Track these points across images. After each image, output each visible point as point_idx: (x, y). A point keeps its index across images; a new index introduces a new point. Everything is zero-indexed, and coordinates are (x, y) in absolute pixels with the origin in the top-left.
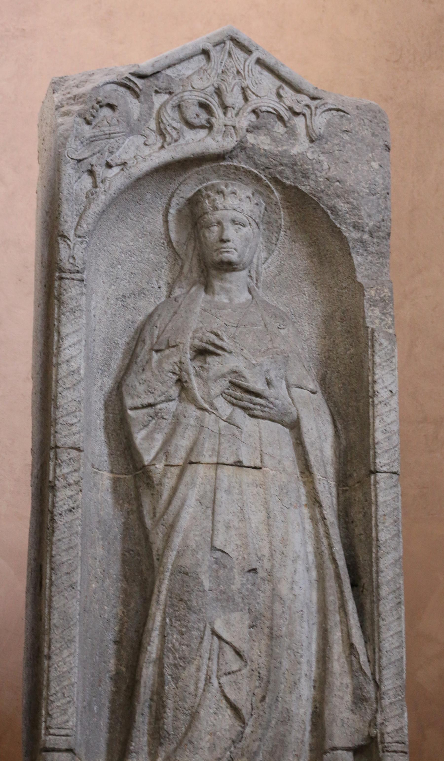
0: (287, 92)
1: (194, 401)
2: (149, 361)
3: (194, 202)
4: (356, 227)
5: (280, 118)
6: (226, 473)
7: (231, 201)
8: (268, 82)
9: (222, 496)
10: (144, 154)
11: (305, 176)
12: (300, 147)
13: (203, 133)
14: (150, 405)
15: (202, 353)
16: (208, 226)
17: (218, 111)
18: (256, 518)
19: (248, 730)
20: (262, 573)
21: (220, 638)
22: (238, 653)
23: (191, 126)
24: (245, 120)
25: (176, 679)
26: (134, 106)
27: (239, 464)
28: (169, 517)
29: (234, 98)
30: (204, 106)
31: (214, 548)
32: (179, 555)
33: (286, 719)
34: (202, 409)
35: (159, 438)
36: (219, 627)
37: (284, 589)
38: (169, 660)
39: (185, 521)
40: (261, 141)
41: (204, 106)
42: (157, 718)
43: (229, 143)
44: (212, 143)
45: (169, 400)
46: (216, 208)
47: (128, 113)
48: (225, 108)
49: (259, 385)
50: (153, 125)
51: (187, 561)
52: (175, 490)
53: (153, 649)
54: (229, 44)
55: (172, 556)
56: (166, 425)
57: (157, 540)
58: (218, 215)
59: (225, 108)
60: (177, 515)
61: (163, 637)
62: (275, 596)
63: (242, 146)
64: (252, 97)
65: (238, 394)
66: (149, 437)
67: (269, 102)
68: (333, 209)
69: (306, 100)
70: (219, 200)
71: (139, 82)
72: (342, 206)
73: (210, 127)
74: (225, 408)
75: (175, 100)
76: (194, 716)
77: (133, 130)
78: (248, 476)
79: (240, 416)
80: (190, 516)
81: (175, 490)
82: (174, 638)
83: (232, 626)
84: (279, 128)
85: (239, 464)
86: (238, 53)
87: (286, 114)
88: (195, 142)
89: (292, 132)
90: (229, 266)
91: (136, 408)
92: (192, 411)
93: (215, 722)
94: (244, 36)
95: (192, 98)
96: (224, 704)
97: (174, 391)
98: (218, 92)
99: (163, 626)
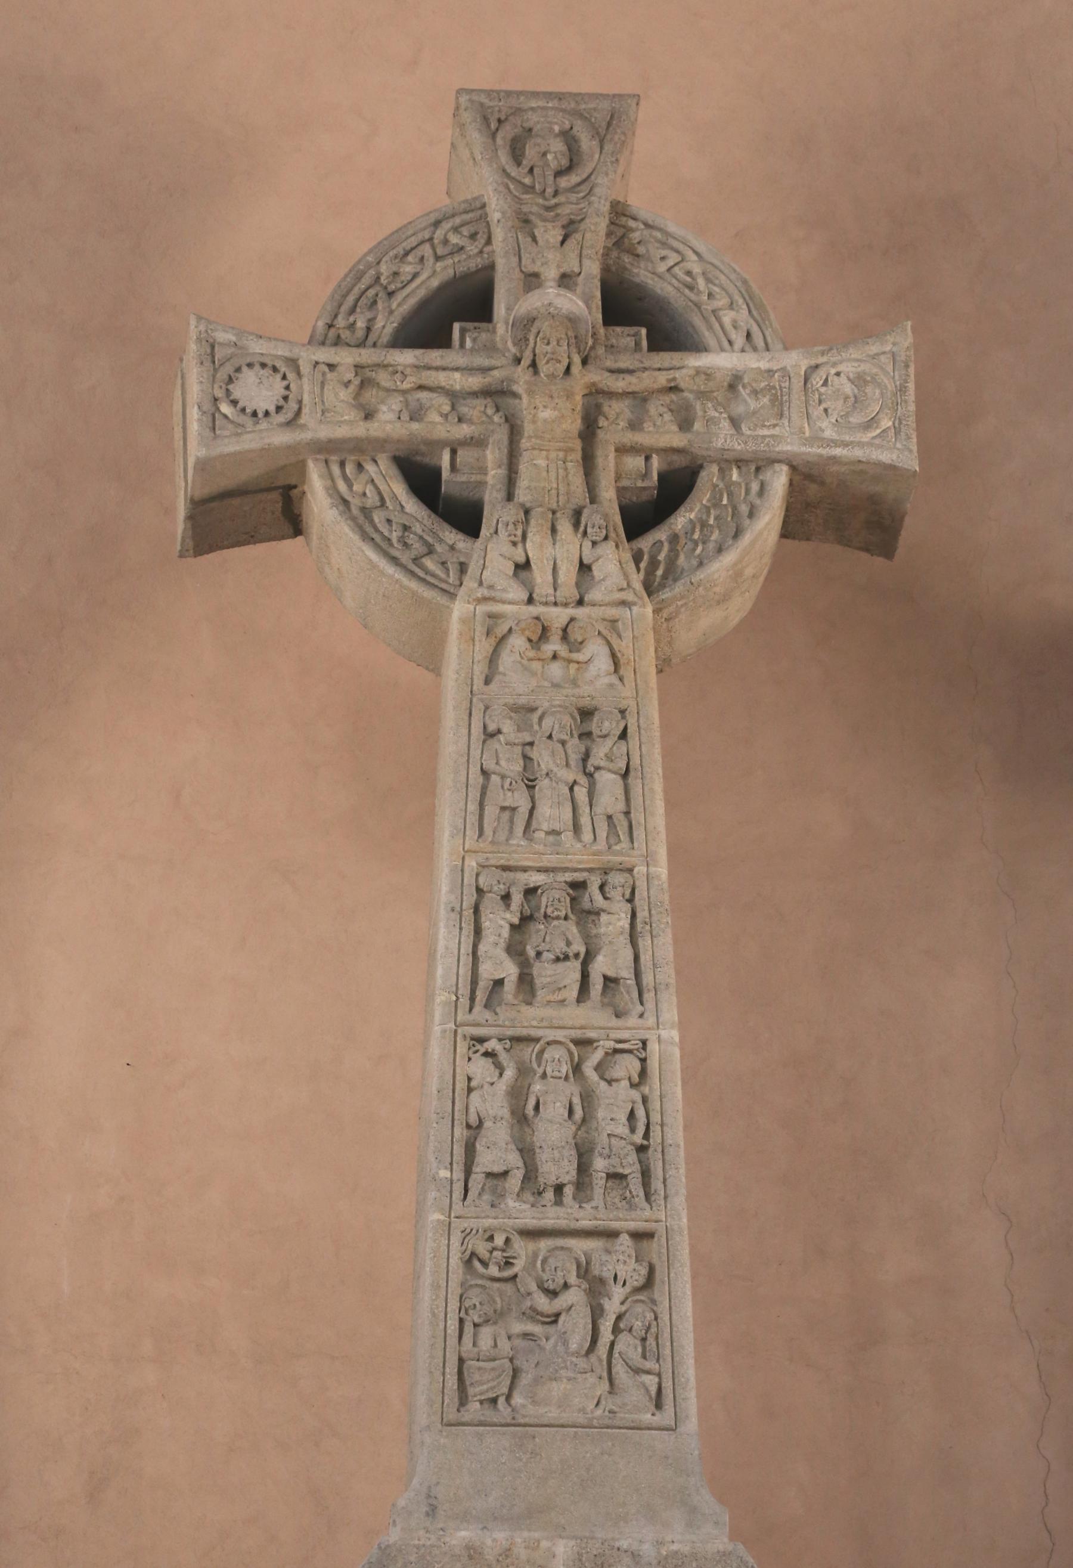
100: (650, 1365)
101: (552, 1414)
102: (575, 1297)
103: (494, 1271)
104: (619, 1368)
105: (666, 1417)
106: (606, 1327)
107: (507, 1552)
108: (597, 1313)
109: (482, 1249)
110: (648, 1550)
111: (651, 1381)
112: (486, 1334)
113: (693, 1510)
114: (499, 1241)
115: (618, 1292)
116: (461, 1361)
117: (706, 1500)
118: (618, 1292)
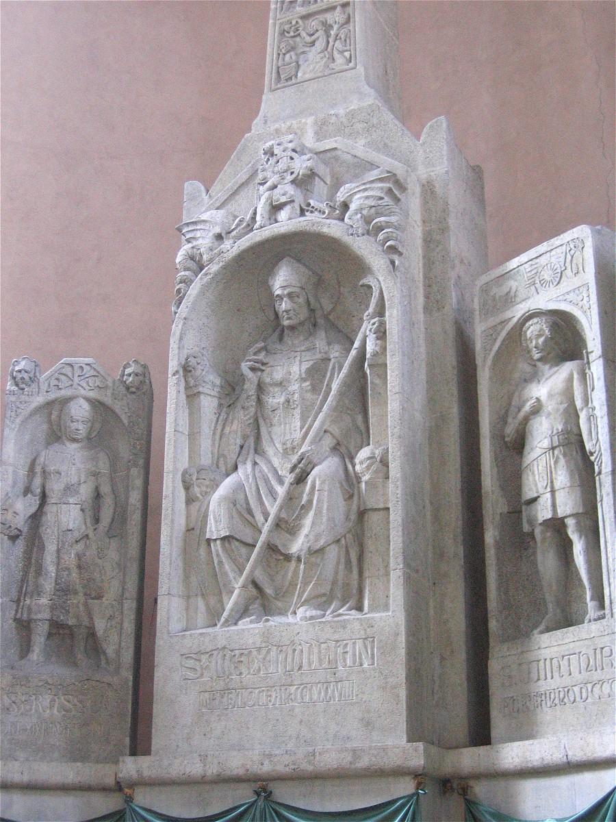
100: (348, 48)
101: (307, 76)
102: (320, 33)
103: (292, 34)
104: (335, 52)
105: (351, 65)
106: (331, 40)
107: (289, 128)
108: (328, 36)
109: (286, 27)
110: (342, 112)
111: (347, 54)
112: (288, 56)
113: (361, 93)
114: (294, 22)
115: (336, 27)
116: (278, 68)
117: (366, 89)
118: (336, 27)
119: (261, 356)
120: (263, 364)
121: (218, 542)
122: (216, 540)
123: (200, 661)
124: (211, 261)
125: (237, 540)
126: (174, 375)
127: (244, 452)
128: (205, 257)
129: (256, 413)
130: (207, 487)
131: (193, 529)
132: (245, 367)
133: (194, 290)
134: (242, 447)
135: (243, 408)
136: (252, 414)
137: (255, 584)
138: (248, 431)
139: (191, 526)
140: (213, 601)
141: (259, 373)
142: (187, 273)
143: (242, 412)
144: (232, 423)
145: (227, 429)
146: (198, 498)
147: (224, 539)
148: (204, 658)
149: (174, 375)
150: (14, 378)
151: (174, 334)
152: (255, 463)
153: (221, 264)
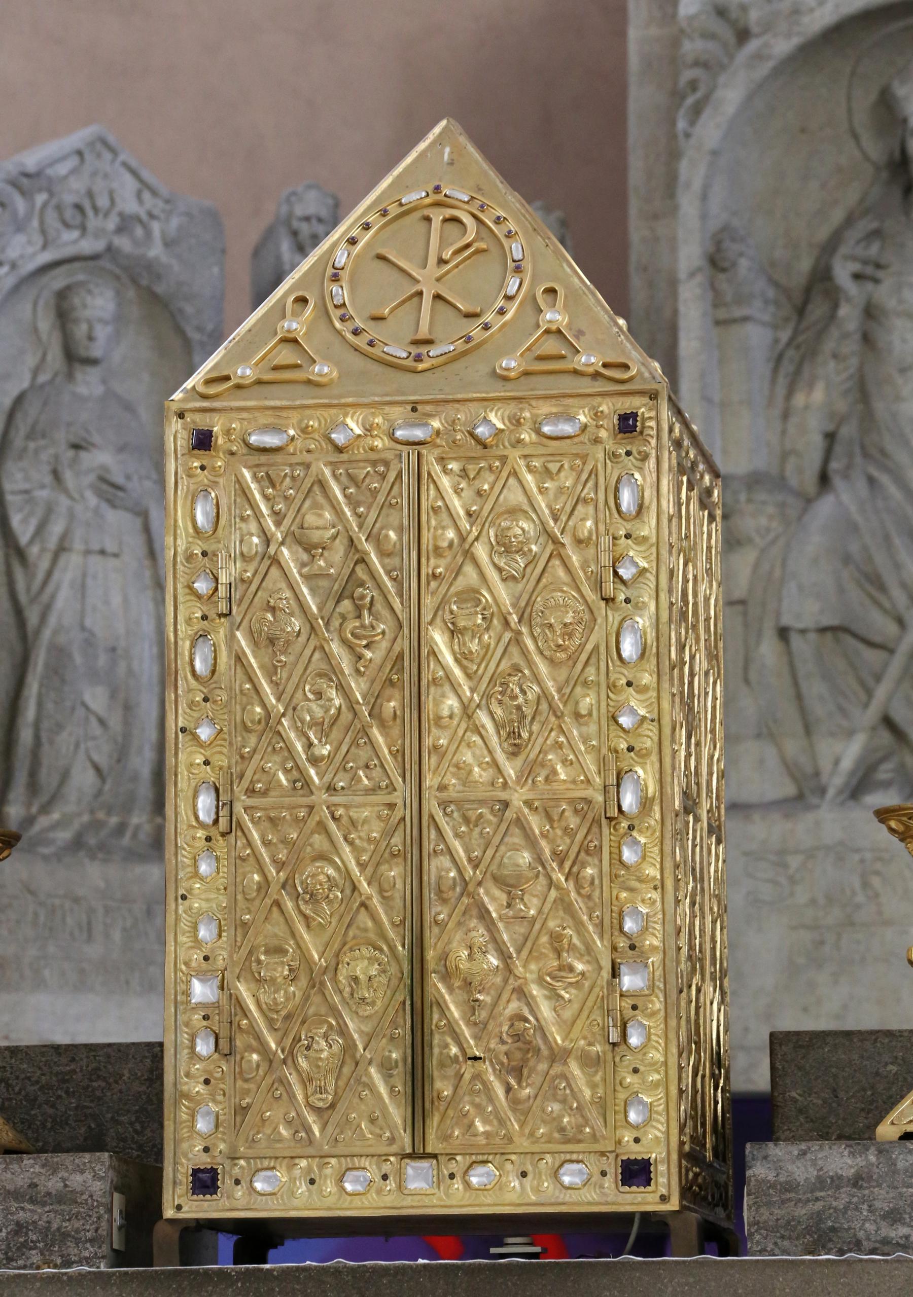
0: (146, 195)
1: (66, 491)
2: (25, 449)
3: (62, 295)
4: (199, 329)
5: (140, 221)
6: (95, 560)
7: (99, 302)
8: (129, 184)
9: (90, 582)
10: (25, 250)
11: (159, 277)
12: (156, 251)
13: (75, 234)
14: (26, 492)
15: (76, 447)
16: (76, 321)
17: (90, 213)
18: (116, 600)
19: (107, 787)
20: (119, 652)
21: (87, 708)
22: (102, 722)
23: (67, 225)
24: (111, 224)
25: (51, 742)
26: (20, 204)
27: (102, 552)
28: (45, 597)
29: (103, 202)
30: (79, 207)
31: (83, 628)
32: (56, 632)
33: (135, 778)
34: (72, 498)
35: (33, 523)
36: (87, 698)
37: (135, 665)
38: (45, 725)
39: (59, 603)
40: (124, 243)
41: (79, 207)
42: (33, 774)
43: (99, 246)
44: (88, 246)
45: (43, 487)
46: (85, 306)
47: (15, 213)
48: (96, 209)
49: (120, 480)
50: (35, 223)
51: (62, 639)
52: (49, 574)
53: (30, 712)
54: (99, 146)
55: (47, 633)
56: (40, 512)
57: (32, 618)
58: (87, 313)
59: (96, 209)
60: (53, 597)
61: (40, 705)
62: (130, 672)
63: (109, 249)
64: (118, 200)
65: (105, 487)
66: (25, 521)
67: (130, 206)
68: (181, 311)
69: (161, 204)
70: (89, 299)
71: (25, 181)
72: (189, 309)
73: (83, 228)
74: (92, 500)
75: (54, 201)
76: (65, 776)
77: (20, 227)
78: (112, 563)
79: (104, 506)
80: (64, 598)
81: (49, 574)
82: (49, 706)
83: (96, 698)
84: (139, 232)
85: (102, 552)
86: (108, 156)
87: (144, 217)
88: (71, 242)
89: (148, 233)
90: (93, 362)
91: (13, 493)
92: (64, 501)
93: (83, 779)
94: (111, 139)
95: (69, 199)
96: (88, 765)
97: (48, 479)
98: (90, 194)
99: (40, 696)
119: (874, 249)
120: (878, 266)
121: (812, 636)
122: (803, 631)
123: (785, 866)
124: (768, 27)
125: (855, 635)
126: (692, 275)
127: (838, 449)
128: (754, 15)
129: (861, 368)
130: (771, 518)
131: (742, 602)
132: (842, 272)
133: (731, 95)
134: (830, 437)
135: (835, 356)
136: (852, 370)
137: (888, 722)
138: (842, 406)
139: (738, 594)
140: (793, 747)
141: (870, 286)
142: (711, 45)
143: (832, 364)
144: (811, 386)
145: (799, 399)
146: (750, 541)
147: (823, 630)
148: (794, 862)
149: (692, 275)
150: (295, 234)
151: (688, 185)
152: (871, 481)
153: (796, 41)
